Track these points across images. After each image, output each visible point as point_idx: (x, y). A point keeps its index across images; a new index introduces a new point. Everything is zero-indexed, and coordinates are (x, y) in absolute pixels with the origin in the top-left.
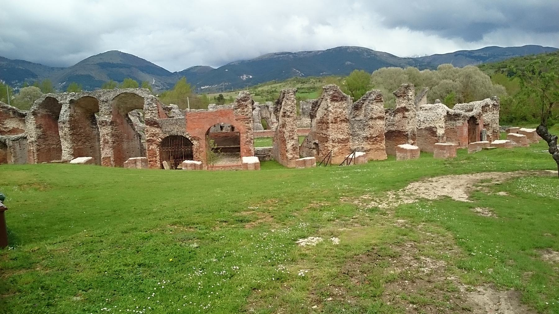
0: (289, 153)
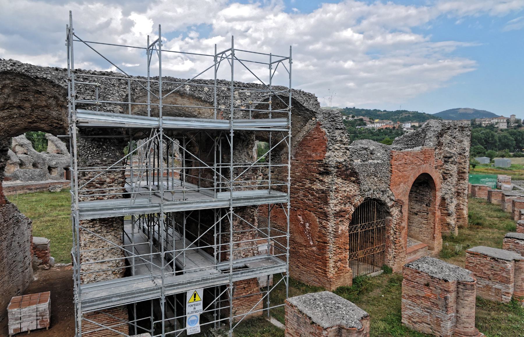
0: (452, 218)
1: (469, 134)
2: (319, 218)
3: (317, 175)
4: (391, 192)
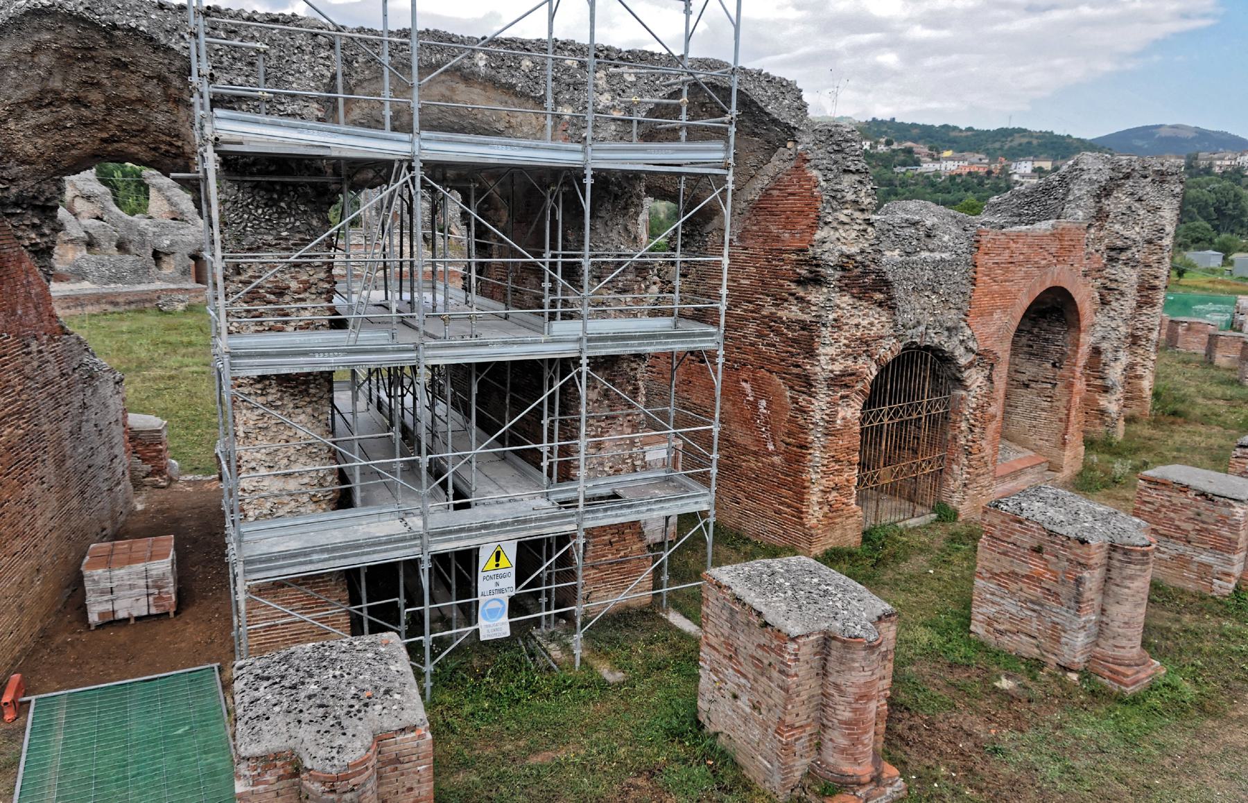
0: (1114, 397)
1: (1178, 190)
2: (792, 388)
3: (793, 286)
4: (970, 332)
